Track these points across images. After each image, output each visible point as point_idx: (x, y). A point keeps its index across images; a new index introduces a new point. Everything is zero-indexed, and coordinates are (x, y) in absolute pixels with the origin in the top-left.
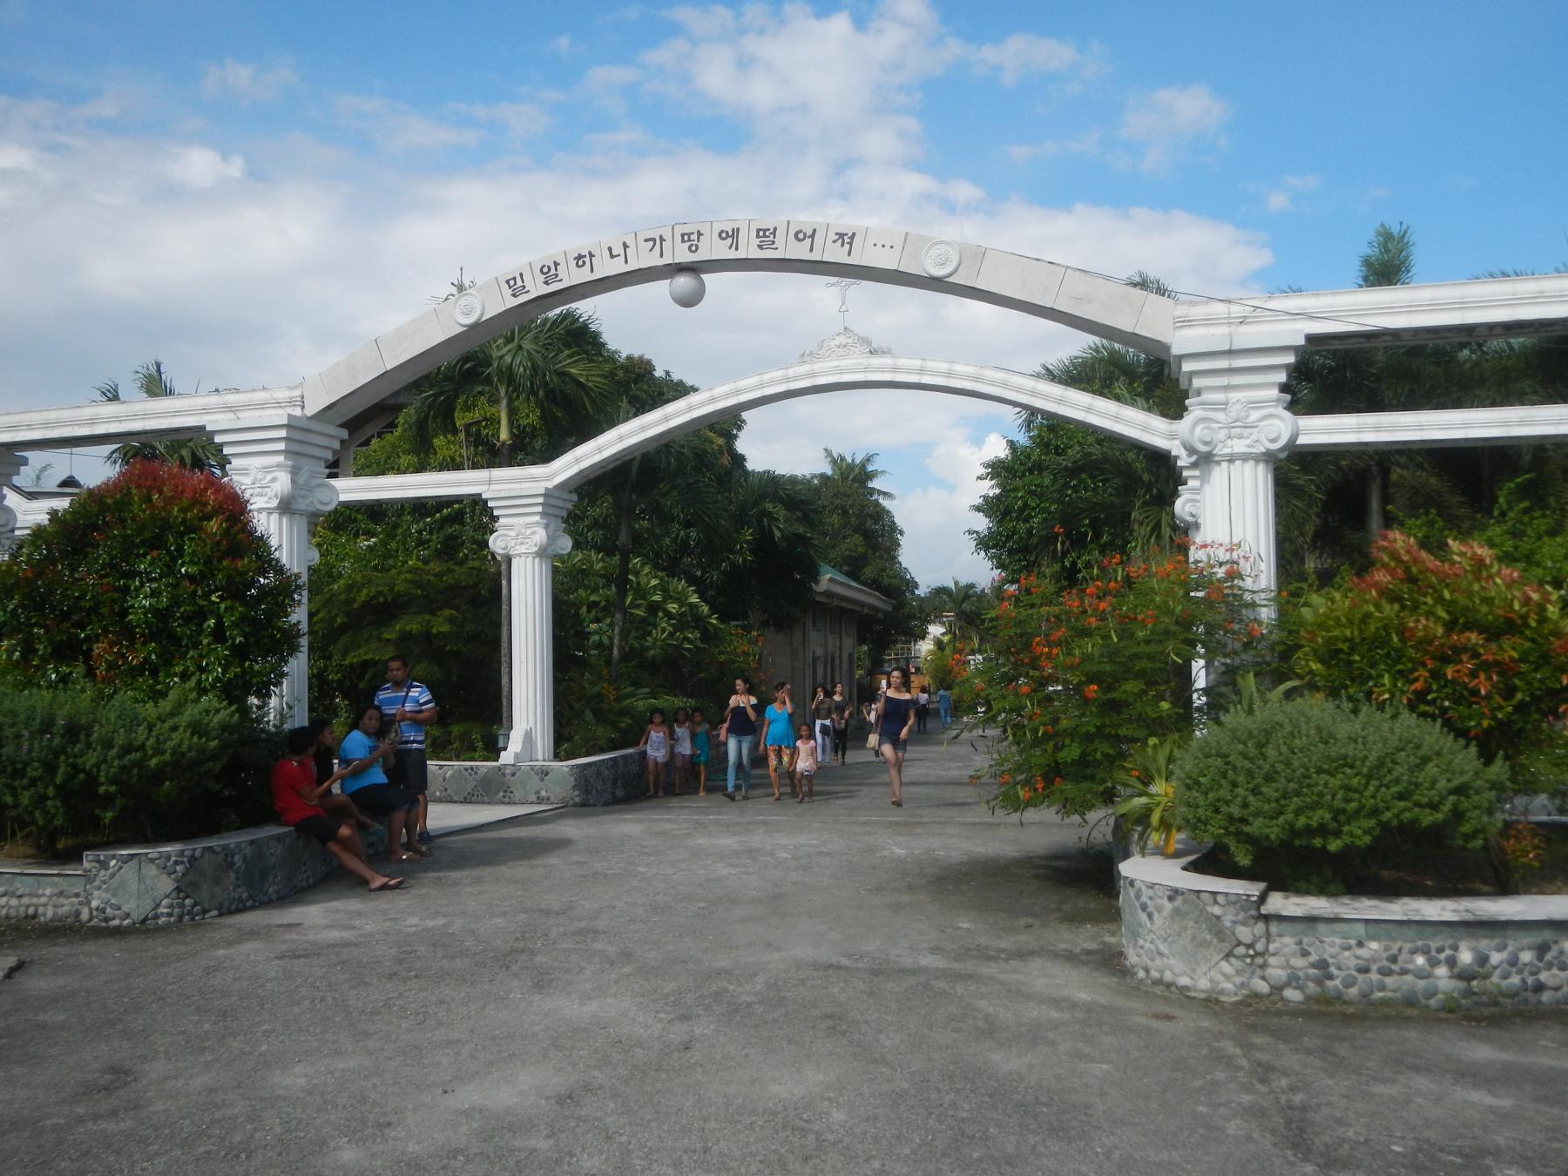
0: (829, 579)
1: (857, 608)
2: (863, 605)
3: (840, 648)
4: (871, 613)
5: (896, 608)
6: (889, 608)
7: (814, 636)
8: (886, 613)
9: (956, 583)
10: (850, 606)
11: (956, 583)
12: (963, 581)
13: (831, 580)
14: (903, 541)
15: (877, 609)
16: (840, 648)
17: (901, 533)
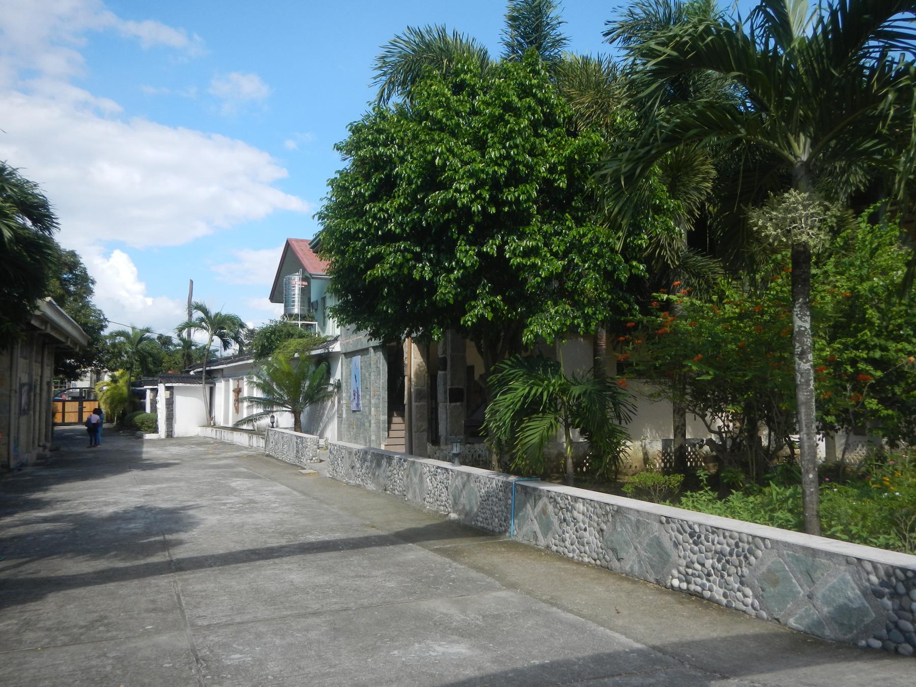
0: (45, 305)
1: (63, 339)
2: (67, 336)
3: (41, 377)
4: (71, 346)
5: (90, 344)
6: (85, 343)
7: (21, 363)
8: (82, 347)
9: (133, 328)
10: (57, 336)
11: (133, 328)
12: (140, 326)
13: (50, 303)
14: (95, 288)
15: (75, 342)
16: (41, 377)
17: (93, 282)
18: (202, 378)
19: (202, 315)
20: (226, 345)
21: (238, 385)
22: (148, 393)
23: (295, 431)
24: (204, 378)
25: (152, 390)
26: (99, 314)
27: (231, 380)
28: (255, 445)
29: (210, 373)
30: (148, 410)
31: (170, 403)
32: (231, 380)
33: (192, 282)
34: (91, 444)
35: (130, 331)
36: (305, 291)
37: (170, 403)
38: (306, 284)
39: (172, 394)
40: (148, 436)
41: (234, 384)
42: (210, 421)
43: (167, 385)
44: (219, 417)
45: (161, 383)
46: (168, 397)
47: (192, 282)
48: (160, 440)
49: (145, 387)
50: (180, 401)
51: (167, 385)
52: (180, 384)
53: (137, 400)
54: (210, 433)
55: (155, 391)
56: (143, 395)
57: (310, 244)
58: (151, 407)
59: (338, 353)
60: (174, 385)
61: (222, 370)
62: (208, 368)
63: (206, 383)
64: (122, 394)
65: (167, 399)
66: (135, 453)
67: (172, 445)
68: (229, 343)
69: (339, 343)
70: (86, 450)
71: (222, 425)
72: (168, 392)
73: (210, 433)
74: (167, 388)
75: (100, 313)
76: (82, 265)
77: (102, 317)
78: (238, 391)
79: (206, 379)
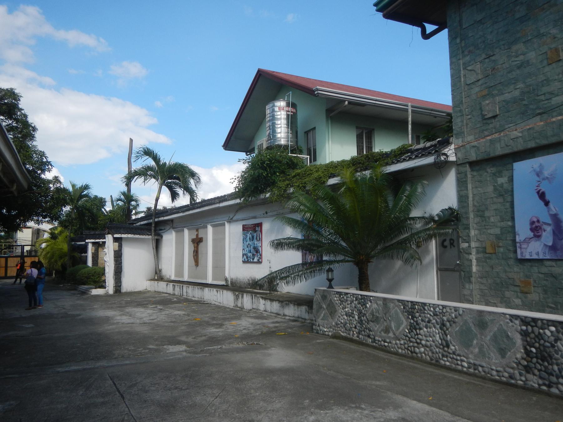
6: (25, 184)
9: (73, 186)
11: (73, 186)
14: (37, 135)
18: (151, 230)
19: (151, 162)
20: (174, 196)
21: (197, 235)
22: (90, 246)
23: (361, 289)
24: (153, 228)
25: (94, 243)
26: (41, 156)
27: (186, 231)
28: (262, 307)
29: (158, 224)
30: (90, 263)
31: (118, 256)
32: (186, 231)
33: (131, 140)
34: (30, 305)
35: (71, 189)
36: (292, 121)
37: (118, 256)
38: (294, 111)
39: (120, 246)
40: (96, 292)
41: (189, 235)
42: (158, 276)
43: (116, 236)
44: (169, 270)
45: (109, 233)
46: (117, 249)
47: (131, 140)
48: (107, 295)
49: (87, 241)
50: (128, 252)
51: (116, 236)
52: (130, 236)
53: (77, 255)
54: (162, 287)
55: (99, 246)
56: (84, 249)
57: (375, 5)
58: (93, 261)
59: (452, 162)
60: (123, 236)
61: (172, 221)
62: (156, 220)
63: (155, 235)
64: (62, 249)
65: (115, 251)
66: (91, 321)
67: (129, 304)
68: (178, 194)
69: (452, 147)
70: (25, 314)
71: (173, 278)
72: (117, 244)
73: (162, 287)
74: (116, 240)
75: (42, 154)
76: (23, 112)
77: (45, 160)
78: (197, 242)
79: (155, 231)
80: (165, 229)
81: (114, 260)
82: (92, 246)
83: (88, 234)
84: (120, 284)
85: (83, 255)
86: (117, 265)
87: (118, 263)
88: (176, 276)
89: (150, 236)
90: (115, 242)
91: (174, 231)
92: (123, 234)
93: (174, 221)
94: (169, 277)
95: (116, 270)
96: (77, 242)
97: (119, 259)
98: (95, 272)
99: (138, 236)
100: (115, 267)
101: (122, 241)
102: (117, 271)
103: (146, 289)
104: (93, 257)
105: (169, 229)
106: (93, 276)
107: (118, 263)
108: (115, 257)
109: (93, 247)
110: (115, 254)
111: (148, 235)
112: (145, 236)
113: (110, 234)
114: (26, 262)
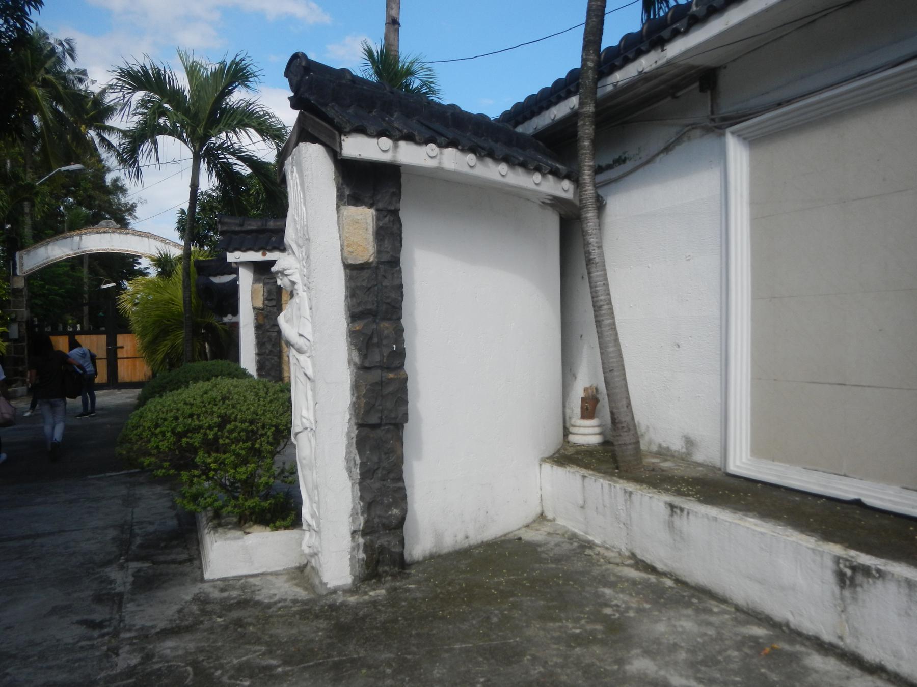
9: (192, 71)
22: (246, 279)
46: (366, 251)
65: (353, 270)
80: (621, 161)
81: (353, 335)
82: (256, 281)
83: (237, 229)
84: (395, 511)
85: (228, 318)
86: (376, 375)
87: (376, 357)
88: (759, 450)
89: (566, 184)
90: (356, 200)
91: (742, 137)
92: (409, 138)
93: (724, 80)
94: (677, 445)
95: (367, 412)
96: (215, 276)
97: (386, 326)
98: (225, 420)
99: (503, 168)
100: (356, 387)
101: (397, 195)
102: (374, 420)
103: (542, 517)
104: (258, 327)
105: (667, 149)
106: (212, 446)
107: (376, 357)
108: (354, 316)
109: (260, 286)
110: (352, 293)
111: (556, 173)
112: (537, 177)
113: (314, 140)
114: (122, 347)
